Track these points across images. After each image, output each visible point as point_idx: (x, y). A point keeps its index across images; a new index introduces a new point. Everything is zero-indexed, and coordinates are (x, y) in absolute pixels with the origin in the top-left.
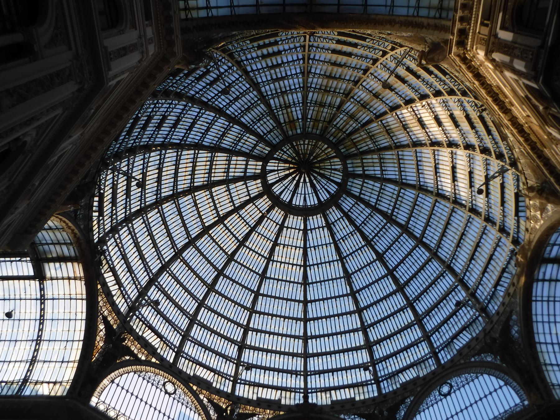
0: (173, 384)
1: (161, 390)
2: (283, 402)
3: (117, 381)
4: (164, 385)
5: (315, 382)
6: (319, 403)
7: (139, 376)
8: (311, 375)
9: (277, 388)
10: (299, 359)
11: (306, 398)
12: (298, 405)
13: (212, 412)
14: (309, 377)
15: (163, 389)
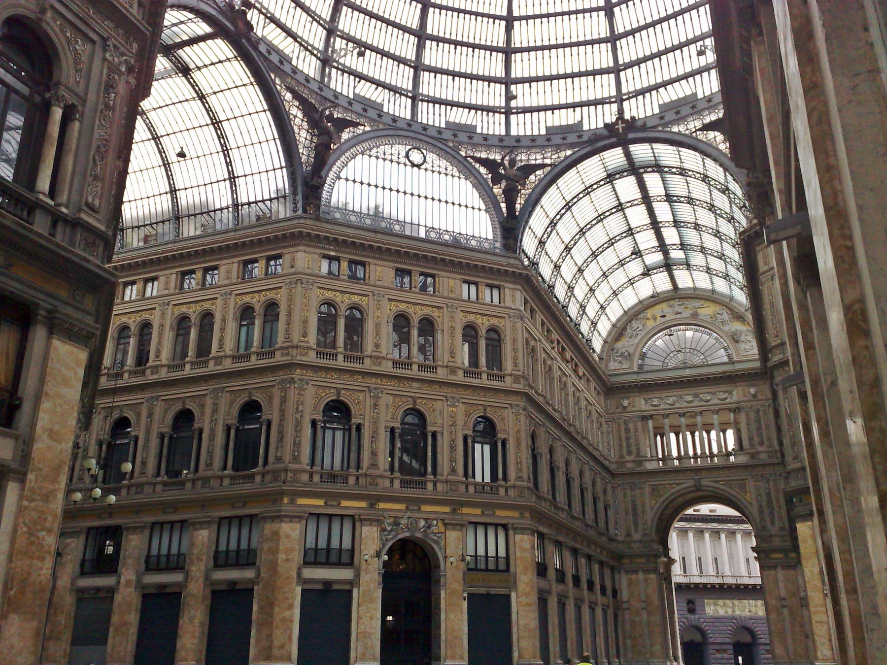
0: (419, 149)
1: (405, 165)
3: (343, 175)
4: (407, 156)
5: (632, 80)
7: (370, 156)
8: (624, 69)
9: (574, 106)
10: (603, 46)
12: (606, 126)
13: (483, 170)
14: (622, 74)
15: (407, 163)
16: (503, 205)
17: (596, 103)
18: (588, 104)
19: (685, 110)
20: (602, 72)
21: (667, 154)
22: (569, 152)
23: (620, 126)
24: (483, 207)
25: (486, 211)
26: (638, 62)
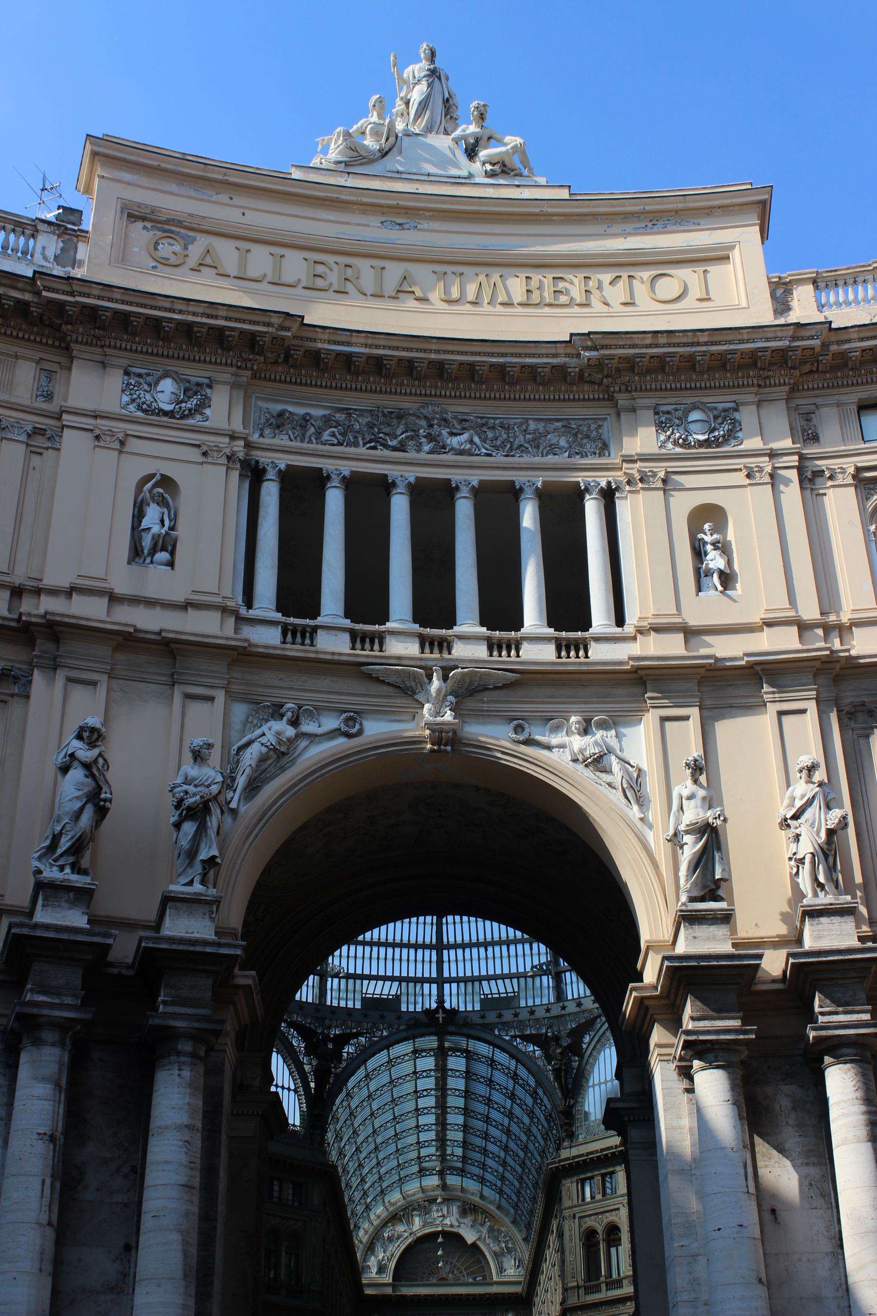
2: (404, 1008)
5: (457, 964)
6: (462, 1009)
9: (392, 979)
11: (441, 1001)
12: (427, 1012)
14: (445, 952)
16: (312, 1085)
17: (416, 980)
18: (408, 980)
19: (508, 1016)
20: (424, 946)
21: (483, 1049)
22: (385, 1034)
23: (440, 1015)
24: (292, 1087)
25: (295, 1091)
26: (463, 946)
